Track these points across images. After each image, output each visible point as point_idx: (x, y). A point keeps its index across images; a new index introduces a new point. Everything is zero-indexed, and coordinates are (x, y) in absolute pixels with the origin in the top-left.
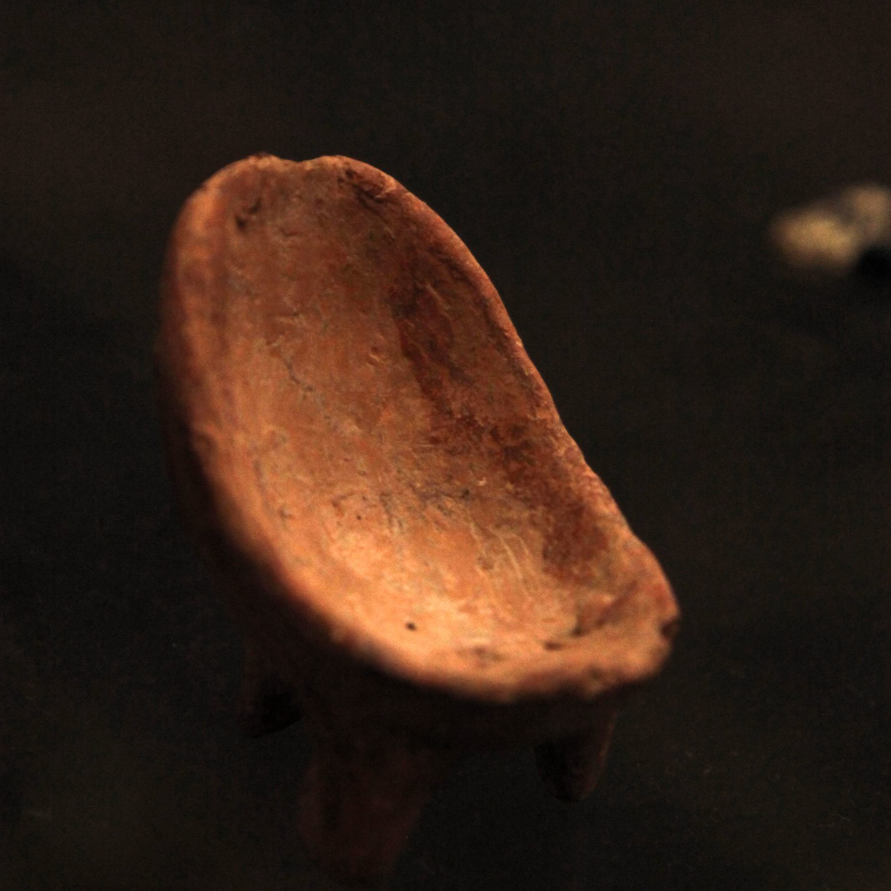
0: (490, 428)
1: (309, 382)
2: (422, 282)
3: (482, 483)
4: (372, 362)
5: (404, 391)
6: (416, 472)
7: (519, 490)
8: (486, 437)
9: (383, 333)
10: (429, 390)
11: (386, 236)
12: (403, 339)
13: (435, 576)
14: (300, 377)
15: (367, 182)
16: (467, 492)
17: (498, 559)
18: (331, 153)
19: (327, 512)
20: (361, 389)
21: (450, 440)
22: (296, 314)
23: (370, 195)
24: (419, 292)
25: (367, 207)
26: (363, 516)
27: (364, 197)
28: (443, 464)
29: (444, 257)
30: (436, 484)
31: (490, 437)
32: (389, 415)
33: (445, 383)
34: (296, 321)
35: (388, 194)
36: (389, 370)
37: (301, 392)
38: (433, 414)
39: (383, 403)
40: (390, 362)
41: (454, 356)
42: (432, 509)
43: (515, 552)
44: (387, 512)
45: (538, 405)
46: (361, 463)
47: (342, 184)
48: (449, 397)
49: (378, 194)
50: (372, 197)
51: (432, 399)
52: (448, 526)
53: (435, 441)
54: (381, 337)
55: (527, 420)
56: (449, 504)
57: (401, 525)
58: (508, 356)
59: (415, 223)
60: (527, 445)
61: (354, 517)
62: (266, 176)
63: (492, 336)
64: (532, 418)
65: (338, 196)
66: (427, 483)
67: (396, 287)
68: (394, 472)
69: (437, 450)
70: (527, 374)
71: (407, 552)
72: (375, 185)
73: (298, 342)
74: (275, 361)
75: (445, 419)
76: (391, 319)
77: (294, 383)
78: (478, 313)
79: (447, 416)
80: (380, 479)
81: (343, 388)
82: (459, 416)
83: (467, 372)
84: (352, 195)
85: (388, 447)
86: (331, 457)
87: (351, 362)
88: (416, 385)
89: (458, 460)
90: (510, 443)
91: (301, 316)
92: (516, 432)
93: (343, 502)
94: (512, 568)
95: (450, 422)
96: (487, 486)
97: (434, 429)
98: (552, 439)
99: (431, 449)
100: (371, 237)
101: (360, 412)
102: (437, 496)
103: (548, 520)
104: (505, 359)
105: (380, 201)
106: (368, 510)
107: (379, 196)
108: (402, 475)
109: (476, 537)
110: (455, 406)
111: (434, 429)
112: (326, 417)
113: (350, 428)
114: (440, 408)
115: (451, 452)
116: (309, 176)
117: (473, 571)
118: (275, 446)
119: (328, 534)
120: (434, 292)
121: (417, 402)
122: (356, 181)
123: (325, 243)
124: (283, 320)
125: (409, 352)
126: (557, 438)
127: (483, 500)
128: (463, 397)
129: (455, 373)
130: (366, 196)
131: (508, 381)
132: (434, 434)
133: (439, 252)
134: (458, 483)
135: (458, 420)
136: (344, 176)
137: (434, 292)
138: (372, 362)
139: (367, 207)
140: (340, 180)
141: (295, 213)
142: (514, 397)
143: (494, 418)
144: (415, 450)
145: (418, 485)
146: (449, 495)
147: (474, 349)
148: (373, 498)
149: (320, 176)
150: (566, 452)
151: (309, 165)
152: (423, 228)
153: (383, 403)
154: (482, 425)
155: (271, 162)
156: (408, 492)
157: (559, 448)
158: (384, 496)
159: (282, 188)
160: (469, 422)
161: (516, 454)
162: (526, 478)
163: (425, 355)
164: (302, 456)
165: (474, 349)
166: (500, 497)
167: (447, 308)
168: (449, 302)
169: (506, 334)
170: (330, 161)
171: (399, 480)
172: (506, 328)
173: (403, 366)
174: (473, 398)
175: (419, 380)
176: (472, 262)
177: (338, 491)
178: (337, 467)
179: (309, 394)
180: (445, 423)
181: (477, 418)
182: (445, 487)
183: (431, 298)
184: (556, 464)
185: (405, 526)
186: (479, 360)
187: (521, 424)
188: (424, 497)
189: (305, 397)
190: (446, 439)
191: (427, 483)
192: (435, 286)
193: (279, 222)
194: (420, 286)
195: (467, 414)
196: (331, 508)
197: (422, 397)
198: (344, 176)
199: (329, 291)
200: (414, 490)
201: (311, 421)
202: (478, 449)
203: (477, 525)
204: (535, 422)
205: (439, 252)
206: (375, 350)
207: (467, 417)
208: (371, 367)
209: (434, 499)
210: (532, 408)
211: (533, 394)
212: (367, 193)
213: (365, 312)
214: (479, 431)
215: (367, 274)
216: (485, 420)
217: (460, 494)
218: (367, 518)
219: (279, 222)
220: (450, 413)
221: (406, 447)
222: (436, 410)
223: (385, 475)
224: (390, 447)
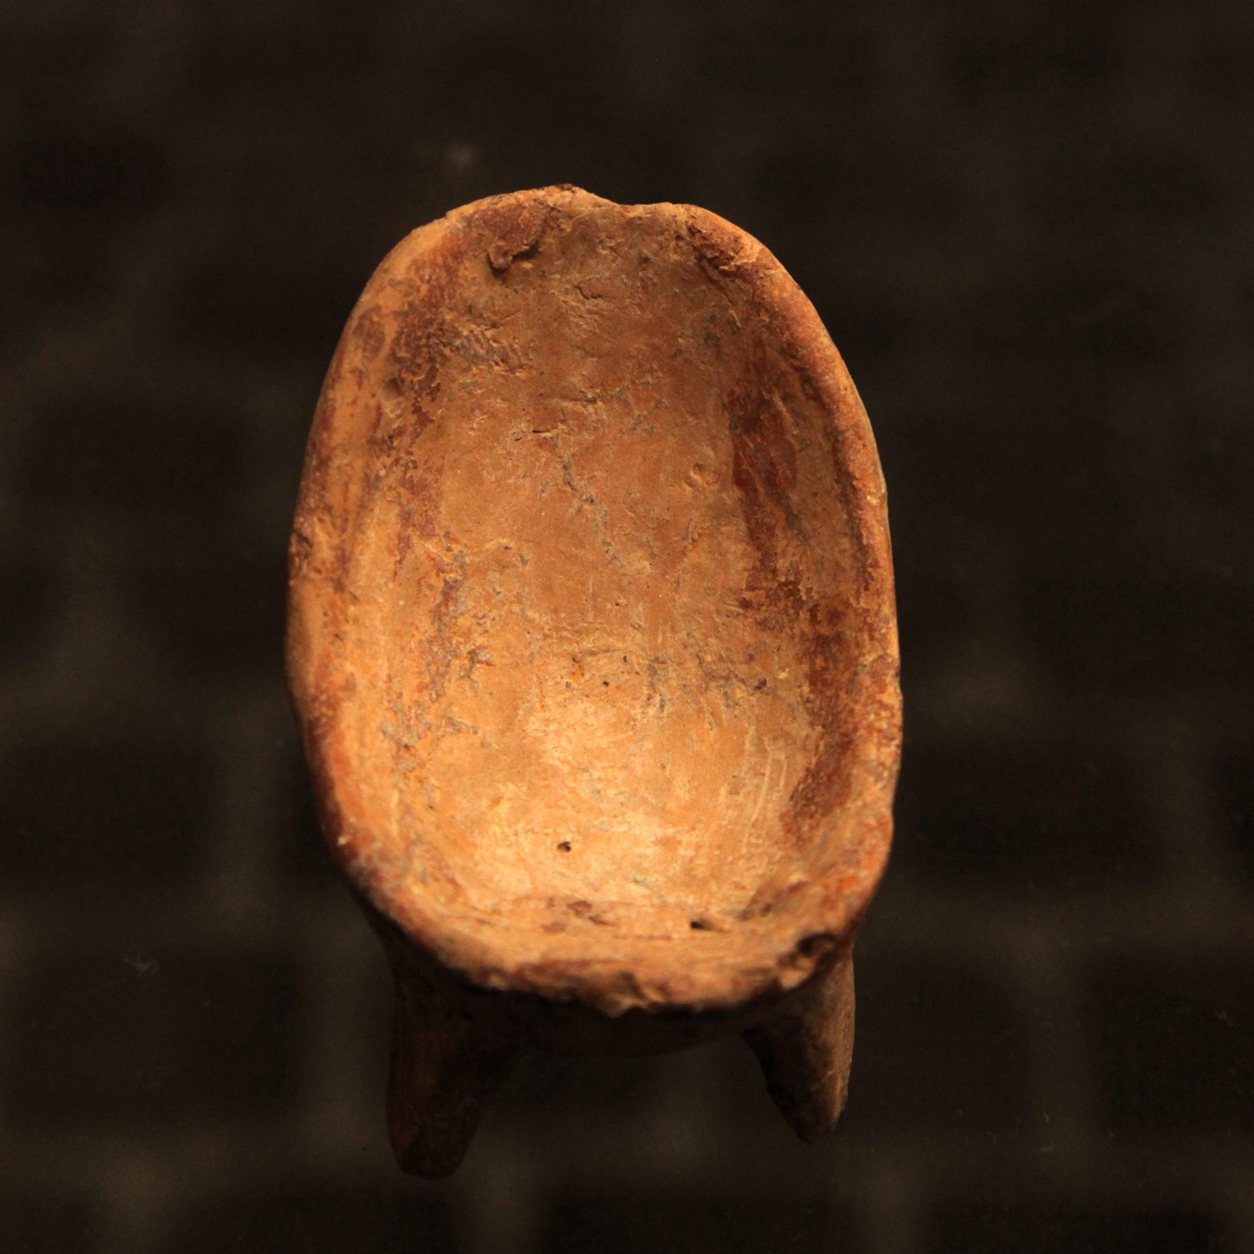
0: (811, 605)
1: (592, 492)
2: (769, 391)
3: (783, 675)
4: (691, 484)
5: (724, 529)
6: (712, 641)
7: (812, 696)
8: (804, 615)
9: (715, 448)
10: (757, 536)
11: (731, 322)
12: (737, 461)
13: (664, 787)
14: (579, 482)
15: (712, 247)
16: (764, 683)
17: (751, 782)
18: (674, 201)
19: (558, 669)
20: (667, 516)
21: (764, 608)
22: (593, 401)
23: (715, 263)
24: (765, 404)
25: (710, 280)
26: (612, 685)
27: (705, 263)
28: (748, 638)
29: (798, 363)
30: (732, 662)
31: (808, 616)
32: (698, 557)
33: (778, 532)
34: (591, 408)
35: (738, 267)
36: (711, 499)
37: (576, 503)
38: (754, 568)
39: (694, 540)
40: (715, 487)
41: (794, 497)
42: (715, 695)
43: (771, 778)
44: (652, 685)
45: (866, 589)
46: (639, 612)
47: (681, 244)
48: (779, 551)
49: (724, 264)
50: (717, 267)
51: (759, 549)
52: (725, 724)
53: (746, 604)
54: (711, 453)
55: (848, 605)
56: (740, 693)
57: (662, 707)
58: (849, 514)
59: (767, 311)
60: (838, 638)
61: (599, 682)
62: (552, 216)
63: (837, 482)
64: (854, 604)
65: (675, 257)
66: (721, 659)
67: (738, 390)
68: (683, 635)
69: (746, 617)
70: (865, 542)
71: (648, 745)
72: (722, 252)
73: (588, 437)
74: (544, 455)
75: (766, 579)
76: (727, 432)
77: (568, 489)
78: (827, 447)
79: (770, 576)
80: (660, 640)
81: (641, 509)
82: (783, 579)
83: (806, 525)
84: (692, 261)
85: (683, 599)
86: (595, 596)
87: (662, 477)
88: (743, 526)
89: (766, 637)
90: (825, 630)
91: (600, 403)
92: (835, 616)
93: (589, 659)
94: (755, 802)
95: (770, 585)
96: (787, 680)
97: (750, 588)
98: (866, 637)
99: (738, 615)
100: (713, 319)
101: (657, 546)
102: (727, 679)
103: (817, 747)
104: (845, 517)
105: (725, 274)
106: (626, 676)
107: (726, 268)
108: (691, 641)
109: (748, 746)
110: (782, 564)
111: (750, 588)
112: (605, 543)
113: (639, 564)
114: (765, 562)
115: (763, 625)
116: (631, 224)
117: (715, 793)
118: (503, 567)
119: (542, 697)
120: (782, 407)
121: (741, 547)
122: (698, 243)
123: (649, 315)
124: (568, 405)
125: (741, 481)
126: (872, 638)
127: (776, 697)
128: (794, 554)
129: (792, 519)
130: (710, 264)
131: (843, 547)
132: (747, 595)
133: (793, 356)
134: (758, 668)
135: (781, 585)
136: (684, 232)
137: (782, 407)
138: (691, 484)
139: (710, 280)
140: (679, 237)
141: (601, 270)
142: (844, 570)
143: (818, 593)
144: (718, 611)
145: (709, 659)
146: (742, 681)
147: (815, 494)
148: (639, 661)
149: (648, 228)
150: (875, 661)
151: (639, 210)
152: (780, 318)
153: (694, 540)
154: (804, 598)
155: (582, 200)
156: (692, 665)
157: (869, 652)
158: (655, 666)
159: (585, 235)
160: (790, 588)
161: (827, 648)
162: (825, 682)
163: (761, 490)
164: (548, 588)
165: (815, 494)
166: (792, 700)
167: (795, 432)
168: (798, 425)
169: (855, 483)
170: (667, 209)
171: (685, 647)
172: (857, 475)
173: (732, 496)
174: (804, 559)
175: (748, 521)
176: (839, 377)
177: (588, 644)
178: (599, 611)
179: (587, 507)
180: (765, 584)
181: (800, 587)
182: (742, 669)
183: (779, 413)
184: (856, 674)
185: (668, 708)
186: (819, 509)
187: (841, 608)
188: (710, 676)
189: (580, 511)
190: (760, 605)
191: (721, 659)
192: (785, 399)
193: (575, 276)
194: (767, 397)
195: (792, 578)
196: (566, 663)
197: (748, 543)
198: (684, 232)
199: (649, 379)
200: (701, 662)
201: (580, 544)
202: (792, 628)
203: (757, 730)
204: (856, 610)
205: (793, 356)
206: (699, 468)
207: (790, 583)
208: (688, 489)
209: (722, 682)
210: (858, 591)
211: (865, 571)
212: (710, 261)
213: (693, 414)
214: (798, 604)
215: (702, 367)
216: (809, 590)
217: (756, 684)
218: (618, 687)
219: (575, 276)
220: (774, 572)
221: (708, 604)
222: (758, 564)
223: (669, 634)
224: (686, 599)
